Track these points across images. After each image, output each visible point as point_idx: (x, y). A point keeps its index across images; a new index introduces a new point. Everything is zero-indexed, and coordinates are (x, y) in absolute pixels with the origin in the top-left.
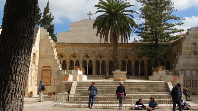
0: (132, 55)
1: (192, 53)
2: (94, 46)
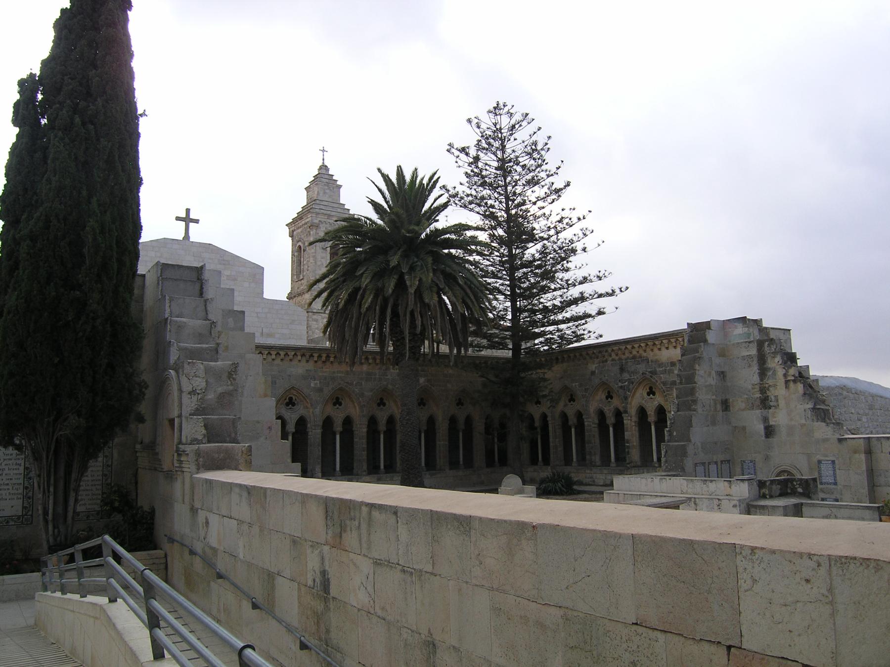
1: (719, 407)
2: (270, 358)
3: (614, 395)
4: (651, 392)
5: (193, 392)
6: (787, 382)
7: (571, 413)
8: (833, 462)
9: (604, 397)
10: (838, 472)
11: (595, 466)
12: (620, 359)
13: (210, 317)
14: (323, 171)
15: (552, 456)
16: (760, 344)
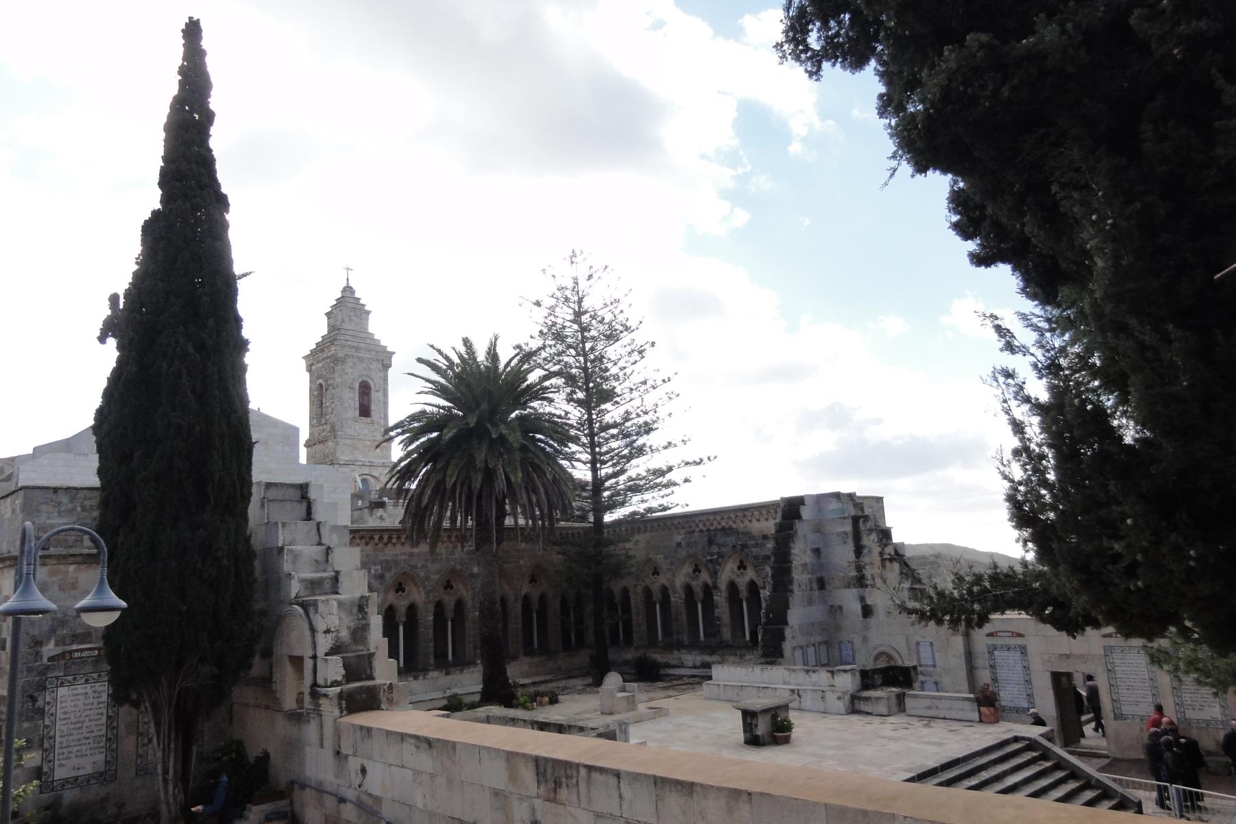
0: (473, 576)
1: (815, 586)
3: (703, 569)
4: (742, 566)
5: (327, 631)
6: (883, 560)
7: (655, 588)
8: (932, 644)
9: (691, 570)
10: (937, 654)
11: (684, 647)
12: (708, 530)
13: (323, 541)
14: (348, 294)
15: (635, 635)
16: (855, 520)
